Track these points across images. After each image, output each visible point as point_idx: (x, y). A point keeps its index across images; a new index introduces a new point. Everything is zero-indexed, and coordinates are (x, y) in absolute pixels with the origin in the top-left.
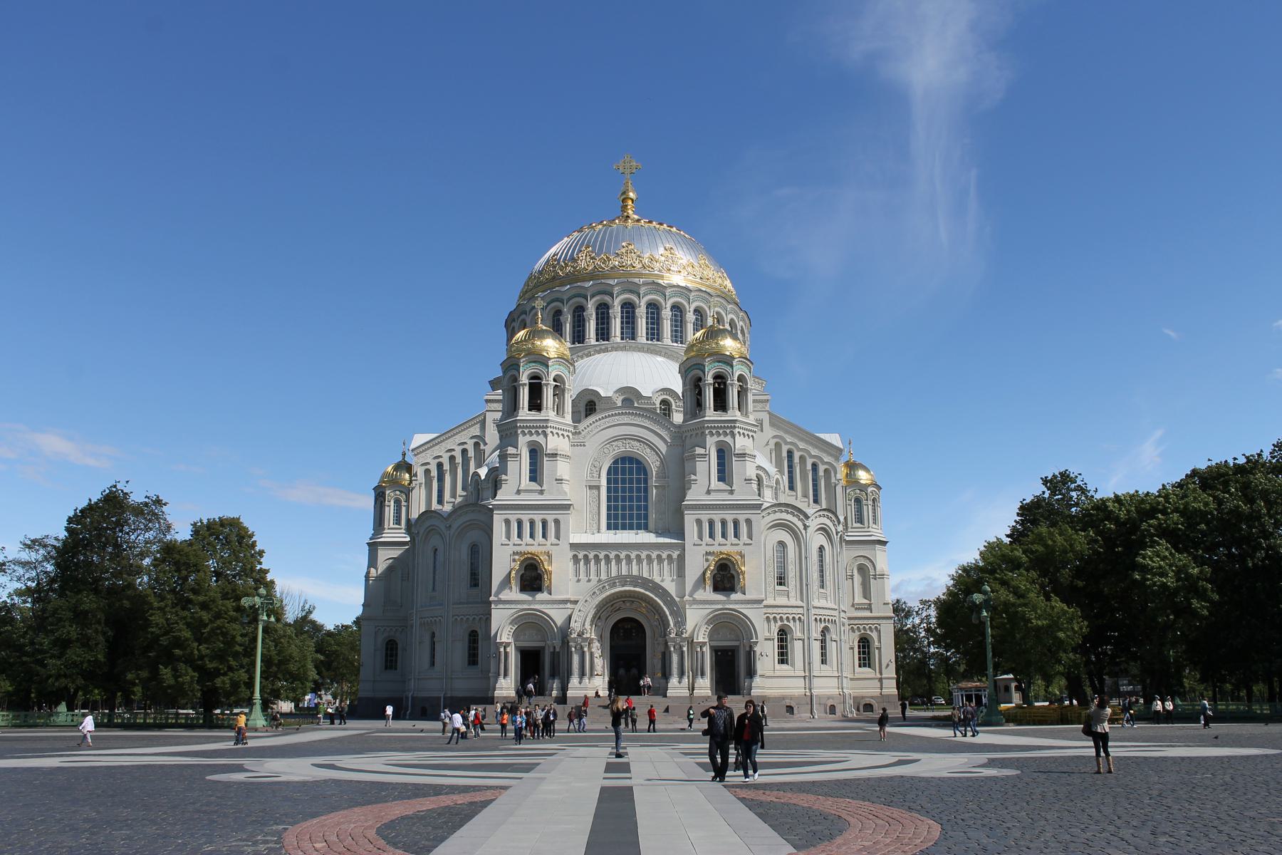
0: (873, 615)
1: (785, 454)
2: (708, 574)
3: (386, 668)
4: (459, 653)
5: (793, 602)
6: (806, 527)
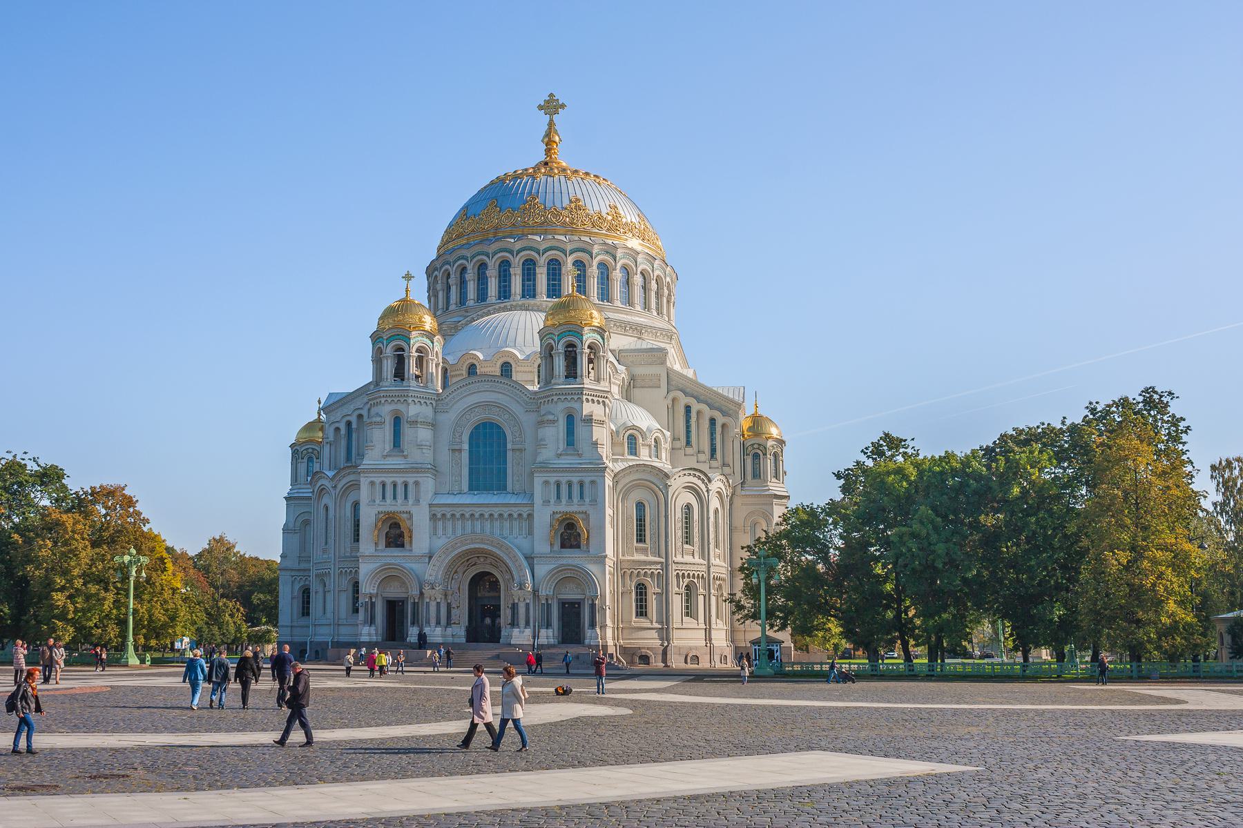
1: (682, 411)
4: (345, 602)
5: (651, 558)
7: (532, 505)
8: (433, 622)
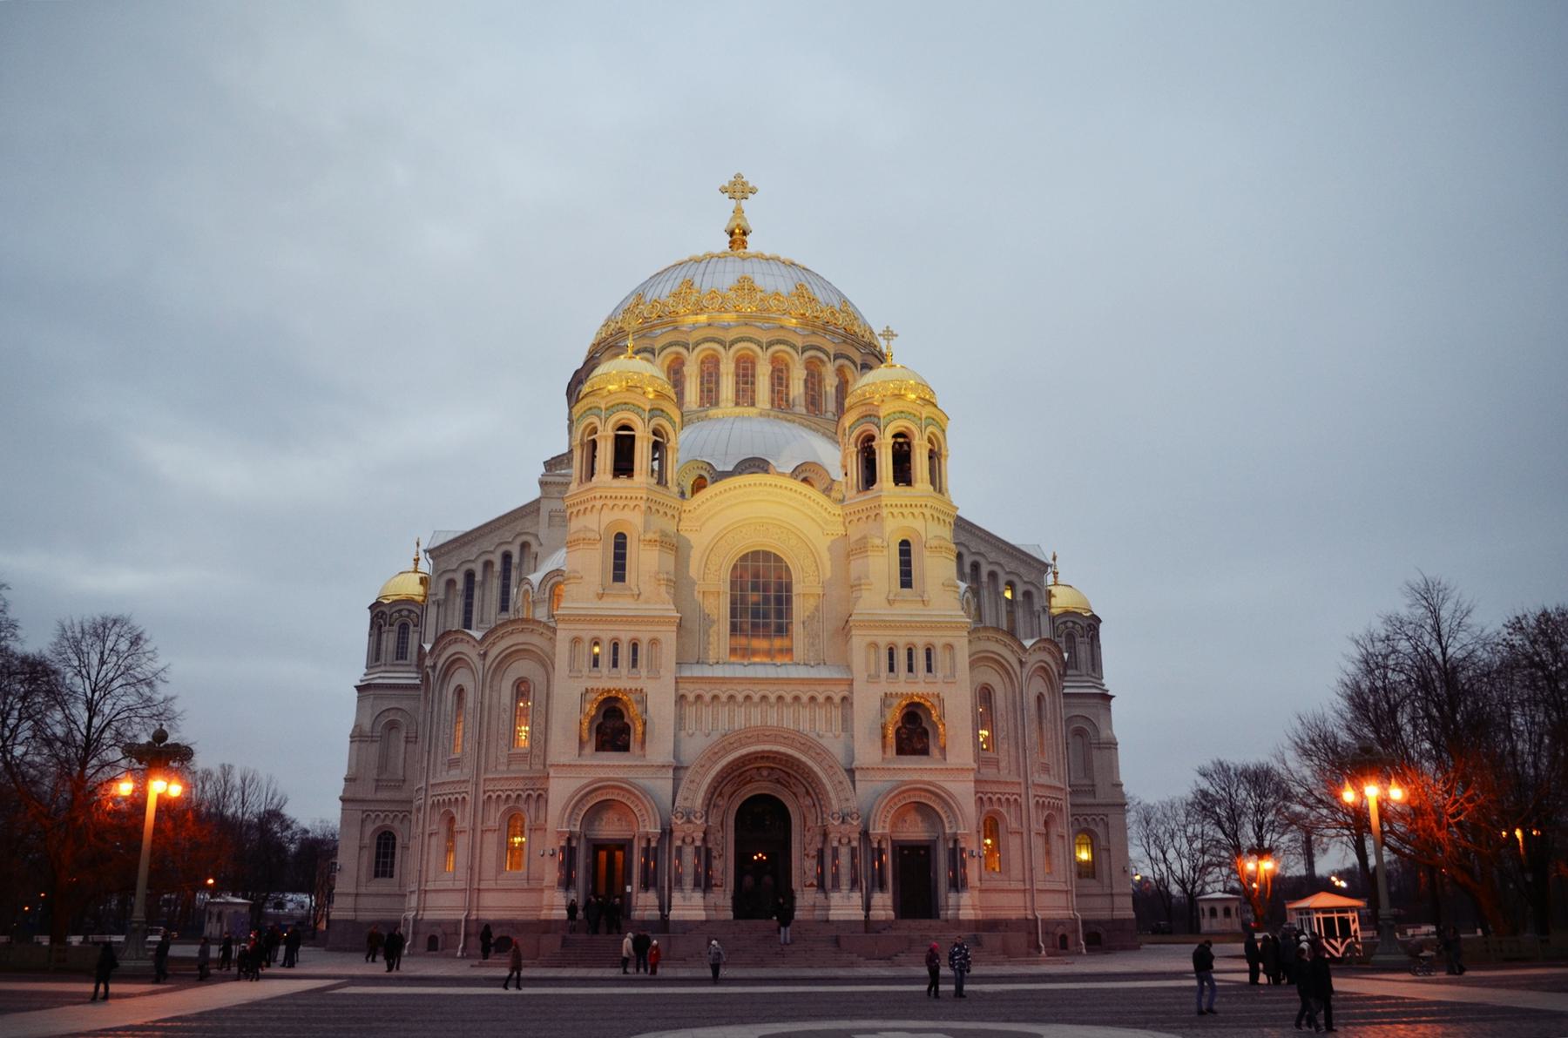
0: (1097, 801)
2: (891, 732)
3: (376, 875)
5: (1004, 775)
6: (1021, 662)
7: (851, 683)
8: (688, 880)
